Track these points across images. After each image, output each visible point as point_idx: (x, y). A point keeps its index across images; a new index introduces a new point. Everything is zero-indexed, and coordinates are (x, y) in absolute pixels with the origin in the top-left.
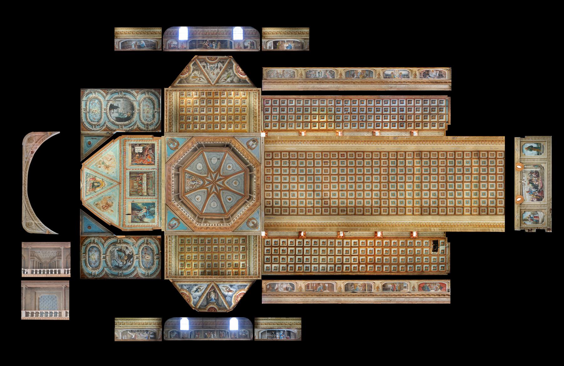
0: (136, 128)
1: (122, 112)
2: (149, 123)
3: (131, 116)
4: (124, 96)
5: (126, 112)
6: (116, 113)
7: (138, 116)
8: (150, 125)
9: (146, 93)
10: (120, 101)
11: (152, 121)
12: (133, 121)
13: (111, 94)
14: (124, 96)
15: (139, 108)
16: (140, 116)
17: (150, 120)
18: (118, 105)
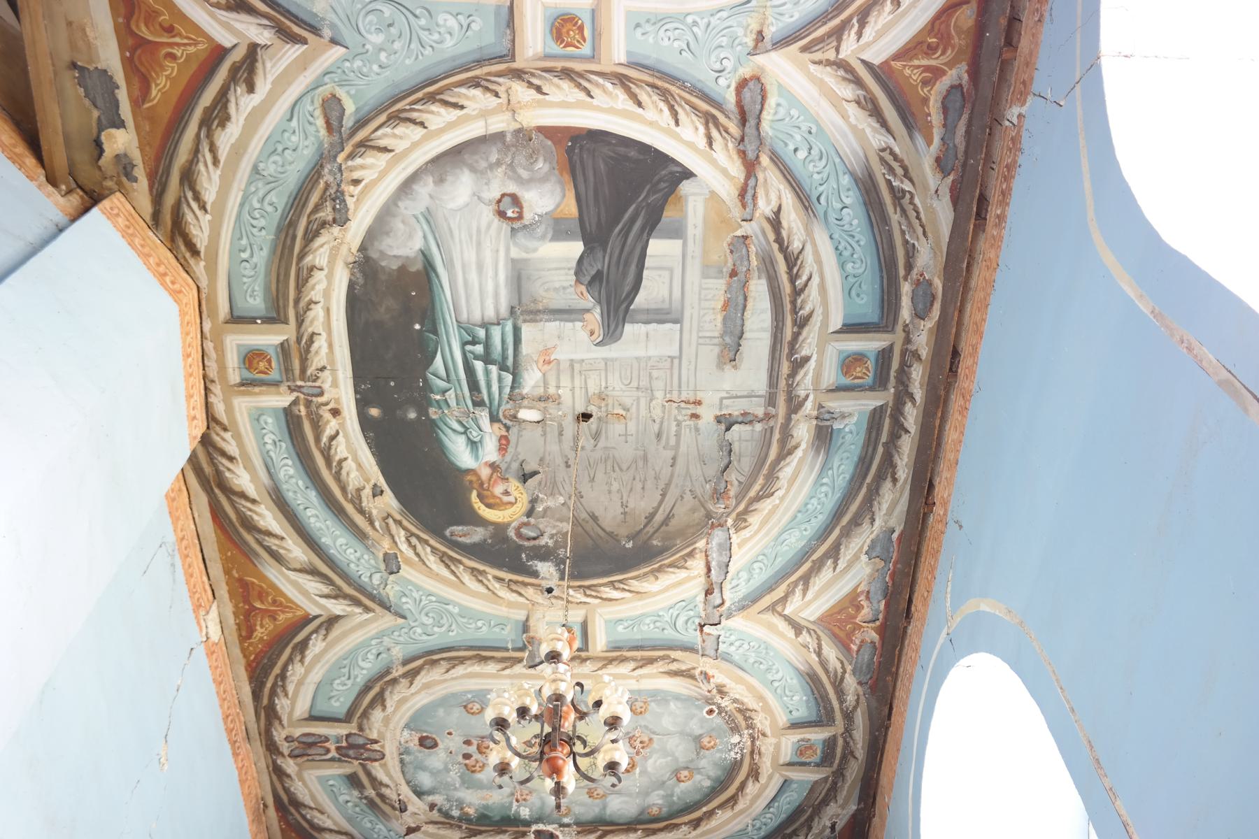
0: (281, 602)
1: (531, 380)
2: (388, 772)
3: (477, 535)
4: (803, 432)
5: (529, 447)
6: (519, 276)
7: (483, 633)
8: (353, 780)
9: (818, 736)
10: (731, 351)
11: (417, 806)
12: (391, 564)
13: (867, 187)
14: (803, 432)
15: (599, 642)
16: (481, 653)
17: (425, 780)
18: (661, 316)
